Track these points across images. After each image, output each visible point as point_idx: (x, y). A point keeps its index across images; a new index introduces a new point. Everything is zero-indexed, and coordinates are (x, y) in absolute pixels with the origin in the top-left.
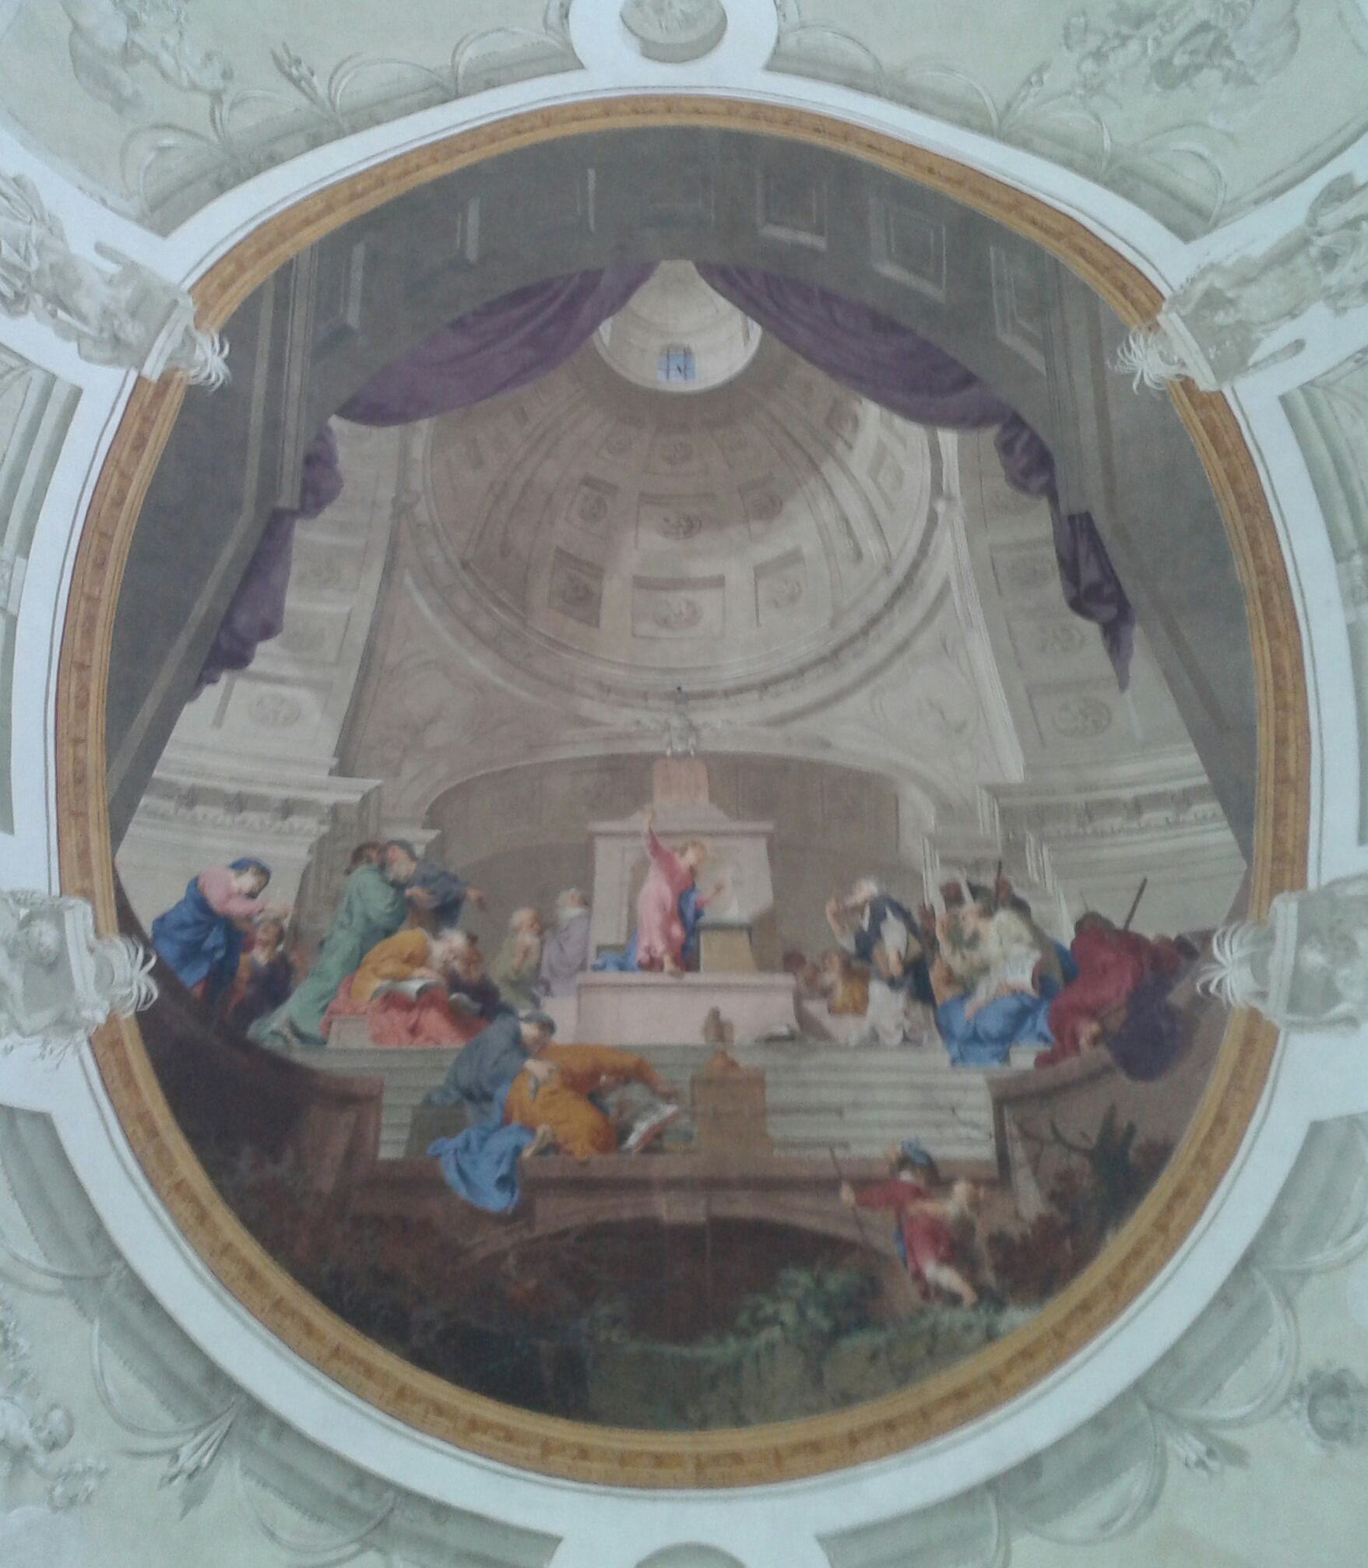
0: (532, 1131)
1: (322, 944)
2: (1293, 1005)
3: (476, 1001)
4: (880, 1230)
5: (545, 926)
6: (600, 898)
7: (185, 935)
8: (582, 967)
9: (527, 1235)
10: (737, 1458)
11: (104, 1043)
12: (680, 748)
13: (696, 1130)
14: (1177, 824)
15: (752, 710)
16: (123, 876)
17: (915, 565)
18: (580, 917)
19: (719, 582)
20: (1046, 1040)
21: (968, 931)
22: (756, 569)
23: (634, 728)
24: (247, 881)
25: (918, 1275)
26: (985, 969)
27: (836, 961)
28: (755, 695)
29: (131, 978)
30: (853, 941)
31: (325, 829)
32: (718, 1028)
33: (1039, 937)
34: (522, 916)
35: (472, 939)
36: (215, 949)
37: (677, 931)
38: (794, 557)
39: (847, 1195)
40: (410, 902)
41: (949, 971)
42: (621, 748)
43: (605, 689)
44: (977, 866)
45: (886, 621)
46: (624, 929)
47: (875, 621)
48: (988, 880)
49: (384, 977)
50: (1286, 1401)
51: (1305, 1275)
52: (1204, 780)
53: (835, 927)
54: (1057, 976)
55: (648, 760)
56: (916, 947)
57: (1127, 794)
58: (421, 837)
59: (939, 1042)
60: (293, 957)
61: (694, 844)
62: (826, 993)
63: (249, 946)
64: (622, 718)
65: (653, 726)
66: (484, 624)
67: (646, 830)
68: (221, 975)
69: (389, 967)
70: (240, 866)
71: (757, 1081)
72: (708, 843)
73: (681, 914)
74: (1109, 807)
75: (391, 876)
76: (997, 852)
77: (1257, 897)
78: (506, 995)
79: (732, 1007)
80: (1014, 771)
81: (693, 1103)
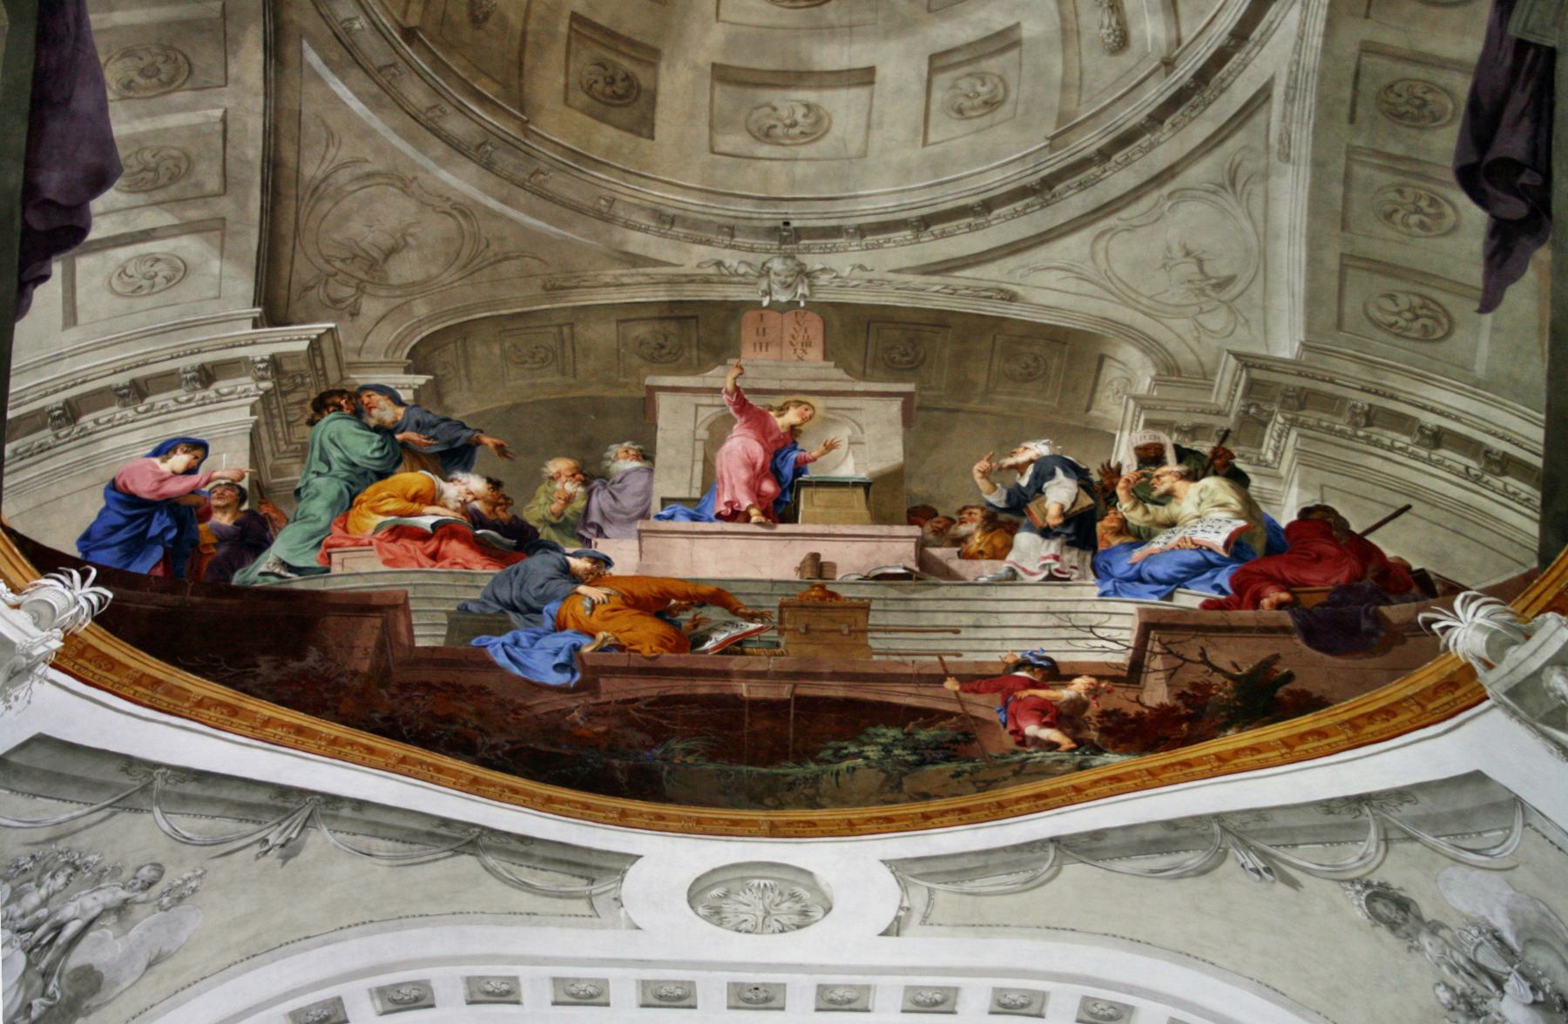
0: (593, 636)
1: (298, 492)
2: (1515, 692)
3: (505, 536)
4: (985, 706)
5: (591, 474)
6: (663, 455)
7: (122, 535)
8: (644, 515)
9: (592, 701)
10: (812, 824)
11: (75, 659)
12: (783, 297)
13: (782, 641)
14: (1477, 480)
15: (900, 253)
16: (20, 529)
17: (1220, 58)
18: (637, 470)
19: (865, 77)
20: (1223, 591)
21: (1162, 489)
22: (933, 58)
23: (712, 270)
24: (180, 460)
25: (1017, 732)
26: (1171, 524)
27: (978, 514)
28: (908, 234)
29: (73, 598)
30: (1004, 497)
31: (267, 385)
32: (817, 567)
33: (1250, 508)
34: (558, 465)
35: (495, 484)
36: (167, 530)
37: (768, 487)
38: (1006, 40)
39: (951, 685)
40: (404, 444)
41: (1124, 521)
42: (690, 293)
43: (665, 220)
44: (1194, 431)
45: (1144, 141)
46: (698, 482)
47: (1125, 140)
48: (1205, 447)
49: (387, 513)
50: (1352, 882)
51: (1412, 839)
52: (1538, 462)
53: (983, 485)
54: (1259, 546)
55: (734, 310)
56: (1087, 501)
57: (1430, 420)
58: (407, 384)
59: (1091, 579)
60: (264, 510)
61: (799, 403)
62: (959, 541)
63: (206, 514)
64: (694, 257)
65: (742, 270)
66: (455, 125)
67: (729, 386)
68: (182, 550)
69: (392, 505)
70: (164, 450)
71: (864, 607)
72: (817, 402)
73: (774, 472)
74: (1401, 422)
75: (373, 422)
76: (1230, 422)
77: (1532, 596)
78: (546, 533)
79: (829, 551)
80: (1286, 344)
81: (781, 621)
